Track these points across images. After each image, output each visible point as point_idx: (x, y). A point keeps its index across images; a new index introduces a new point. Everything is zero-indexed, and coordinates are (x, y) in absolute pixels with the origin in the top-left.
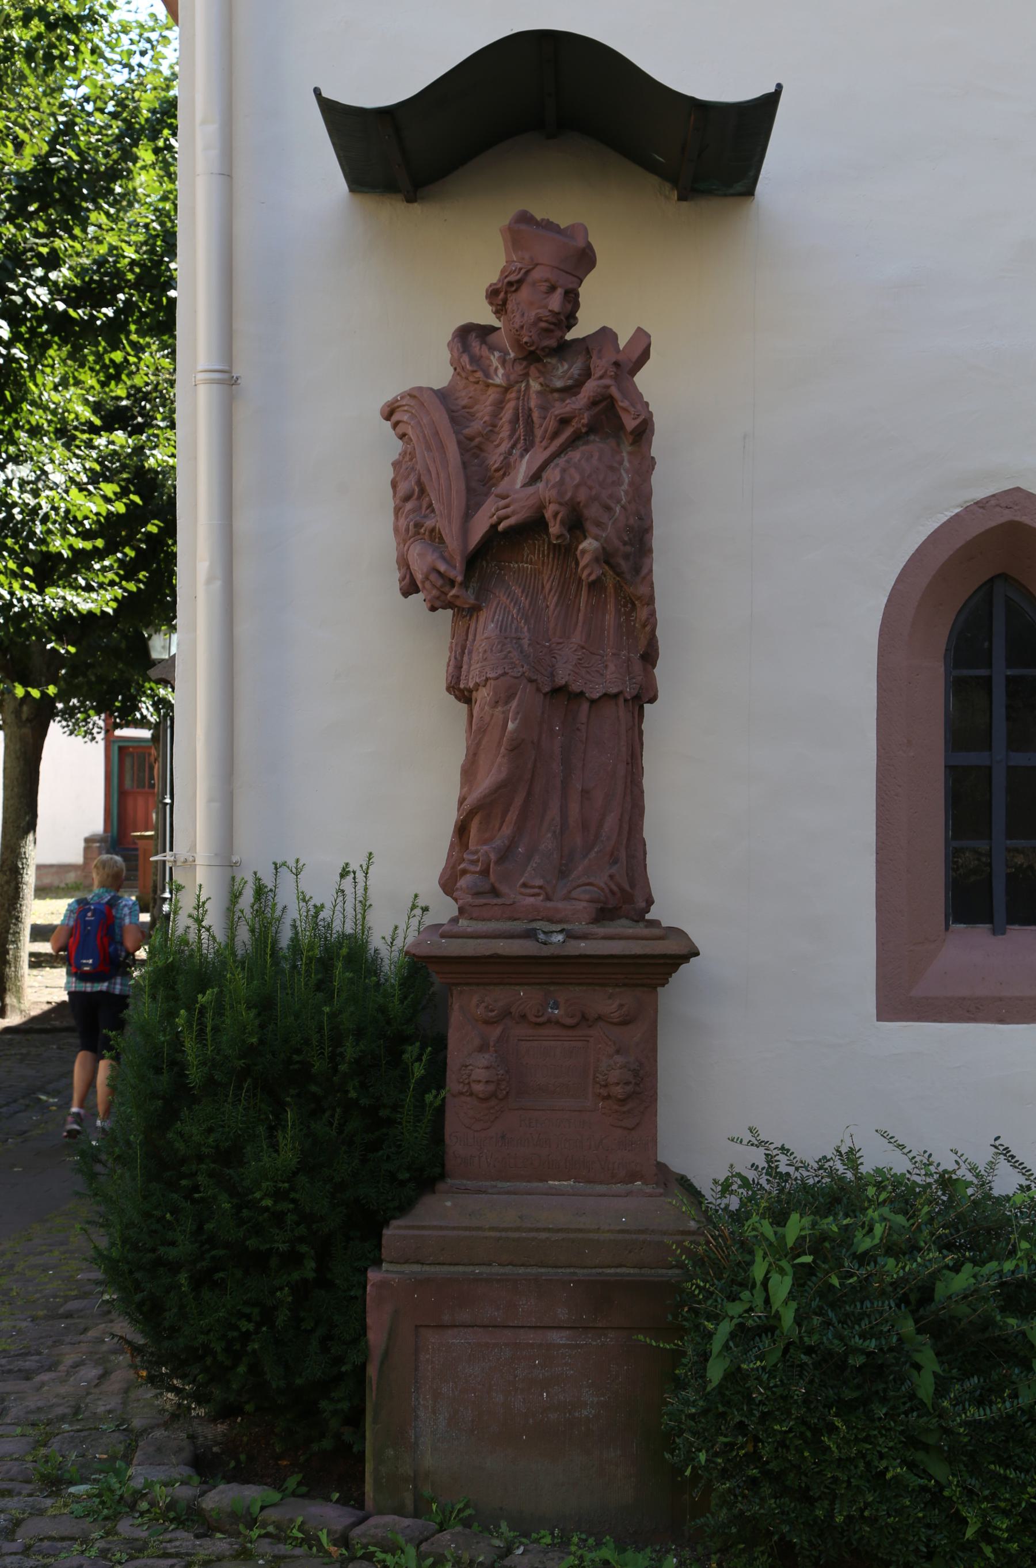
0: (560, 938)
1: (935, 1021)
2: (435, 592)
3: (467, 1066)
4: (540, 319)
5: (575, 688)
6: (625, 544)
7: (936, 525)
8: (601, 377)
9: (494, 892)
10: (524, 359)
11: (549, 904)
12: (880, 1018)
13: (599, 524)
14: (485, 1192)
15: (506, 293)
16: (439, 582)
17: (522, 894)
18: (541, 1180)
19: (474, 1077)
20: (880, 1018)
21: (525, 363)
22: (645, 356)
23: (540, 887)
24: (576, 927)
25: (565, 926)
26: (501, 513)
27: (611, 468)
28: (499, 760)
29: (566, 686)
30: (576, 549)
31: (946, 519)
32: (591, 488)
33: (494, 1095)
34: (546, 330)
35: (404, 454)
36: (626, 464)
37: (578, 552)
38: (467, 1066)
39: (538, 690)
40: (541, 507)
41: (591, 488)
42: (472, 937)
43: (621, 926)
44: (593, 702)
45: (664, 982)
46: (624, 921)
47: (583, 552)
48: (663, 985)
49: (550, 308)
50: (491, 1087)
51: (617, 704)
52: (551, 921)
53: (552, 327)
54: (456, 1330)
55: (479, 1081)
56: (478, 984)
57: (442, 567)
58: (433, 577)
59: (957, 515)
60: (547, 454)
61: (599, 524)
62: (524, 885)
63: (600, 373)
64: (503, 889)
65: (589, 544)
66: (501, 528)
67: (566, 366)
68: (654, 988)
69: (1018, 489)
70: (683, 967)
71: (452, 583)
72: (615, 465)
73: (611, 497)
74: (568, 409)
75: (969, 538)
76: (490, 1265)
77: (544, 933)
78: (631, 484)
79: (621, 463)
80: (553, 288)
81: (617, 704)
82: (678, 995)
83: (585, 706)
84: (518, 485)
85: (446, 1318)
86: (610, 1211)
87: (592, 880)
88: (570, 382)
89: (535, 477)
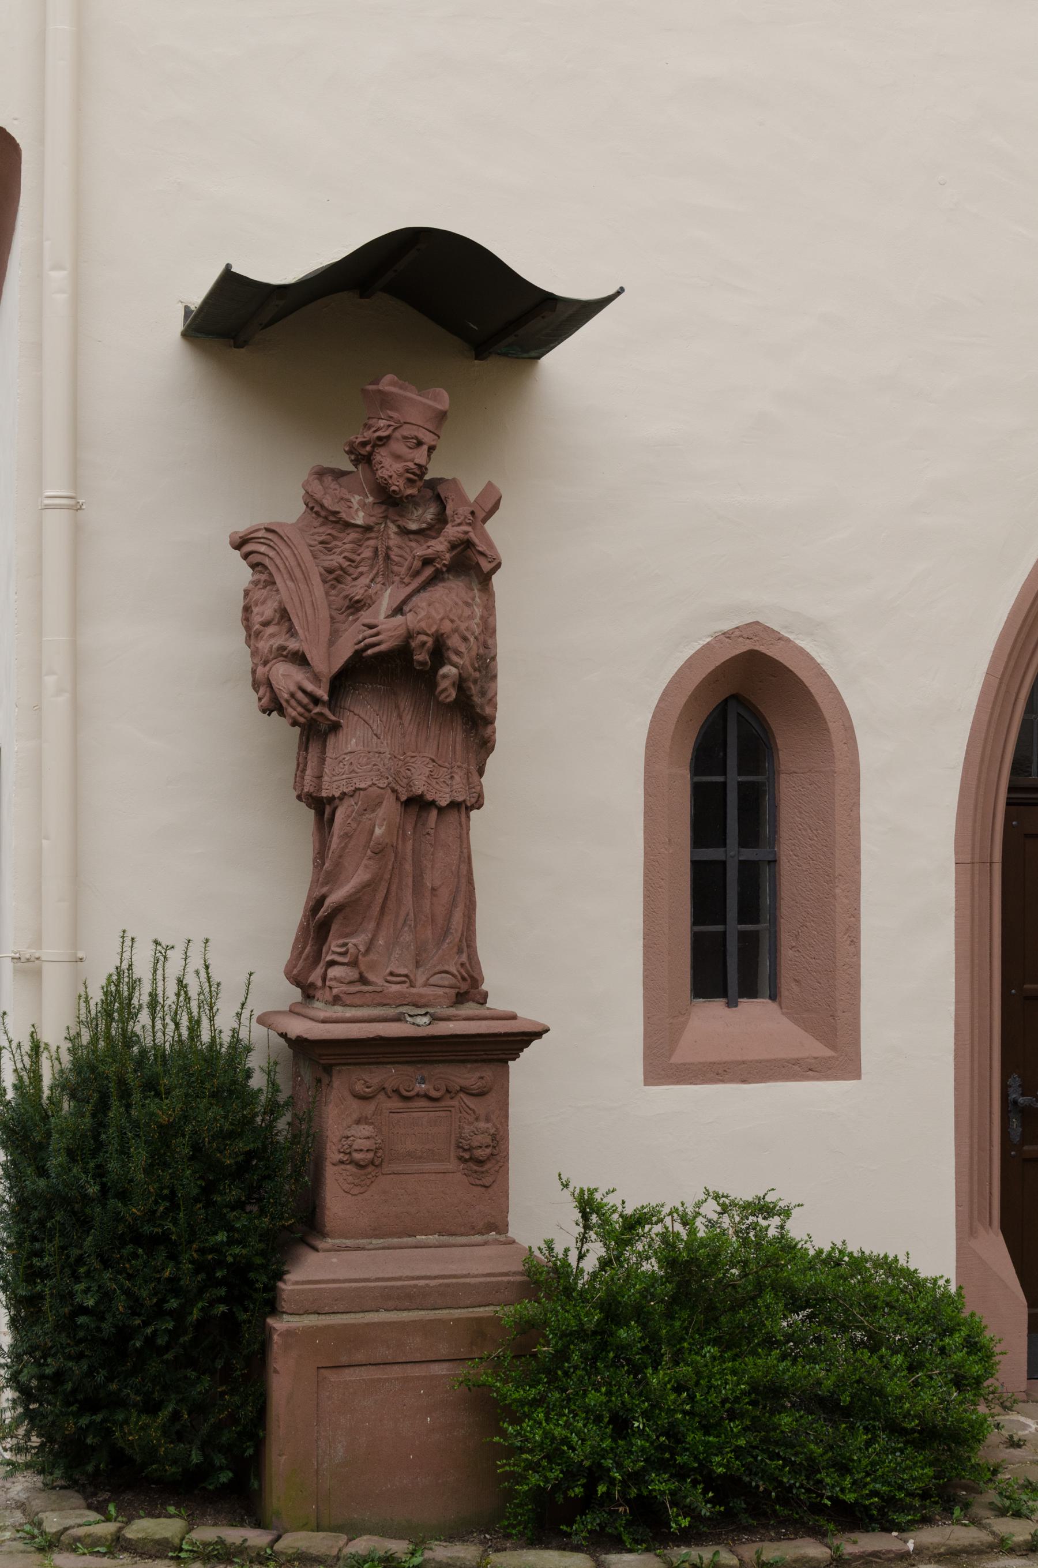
0: (426, 1020)
1: (691, 1084)
2: (300, 709)
3: (348, 1137)
4: (407, 471)
5: (429, 797)
6: (475, 670)
8: (459, 525)
9: (363, 980)
10: (382, 503)
11: (413, 990)
12: (648, 1082)
13: (458, 653)
14: (363, 1249)
15: (373, 447)
16: (305, 700)
17: (388, 982)
18: (410, 1236)
19: (355, 1147)
20: (648, 1082)
21: (384, 507)
22: (496, 507)
23: (406, 976)
24: (438, 1011)
25: (431, 1010)
26: (367, 641)
27: (467, 604)
28: (365, 862)
29: (422, 796)
30: (437, 672)
31: (699, 647)
32: (452, 621)
33: (372, 1163)
34: (410, 480)
35: (256, 583)
36: (477, 599)
37: (438, 678)
38: (348, 1137)
39: (398, 799)
40: (410, 636)
41: (452, 621)
42: (351, 1022)
43: (469, 1009)
44: (441, 810)
45: (515, 1056)
46: (471, 1004)
47: (444, 676)
48: (514, 1059)
49: (417, 461)
50: (370, 1155)
51: (459, 811)
52: (417, 1006)
53: (415, 478)
54: (352, 1369)
55: (361, 1150)
56: (355, 1064)
57: (310, 687)
58: (300, 695)
59: (708, 643)
60: (408, 590)
61: (458, 653)
62: (392, 974)
63: (458, 521)
64: (370, 976)
65: (447, 669)
66: (370, 652)
67: (420, 512)
68: (505, 1062)
69: (757, 623)
70: (535, 1044)
71: (316, 701)
72: (470, 601)
73: (467, 629)
74: (430, 551)
75: (718, 664)
76: (377, 1311)
77: (410, 1016)
78: (482, 617)
79: (473, 599)
80: (420, 443)
81: (459, 811)
82: (522, 1070)
83: (434, 813)
84: (382, 616)
85: (344, 1360)
86: (474, 1261)
87: (446, 968)
88: (424, 525)
89: (399, 610)
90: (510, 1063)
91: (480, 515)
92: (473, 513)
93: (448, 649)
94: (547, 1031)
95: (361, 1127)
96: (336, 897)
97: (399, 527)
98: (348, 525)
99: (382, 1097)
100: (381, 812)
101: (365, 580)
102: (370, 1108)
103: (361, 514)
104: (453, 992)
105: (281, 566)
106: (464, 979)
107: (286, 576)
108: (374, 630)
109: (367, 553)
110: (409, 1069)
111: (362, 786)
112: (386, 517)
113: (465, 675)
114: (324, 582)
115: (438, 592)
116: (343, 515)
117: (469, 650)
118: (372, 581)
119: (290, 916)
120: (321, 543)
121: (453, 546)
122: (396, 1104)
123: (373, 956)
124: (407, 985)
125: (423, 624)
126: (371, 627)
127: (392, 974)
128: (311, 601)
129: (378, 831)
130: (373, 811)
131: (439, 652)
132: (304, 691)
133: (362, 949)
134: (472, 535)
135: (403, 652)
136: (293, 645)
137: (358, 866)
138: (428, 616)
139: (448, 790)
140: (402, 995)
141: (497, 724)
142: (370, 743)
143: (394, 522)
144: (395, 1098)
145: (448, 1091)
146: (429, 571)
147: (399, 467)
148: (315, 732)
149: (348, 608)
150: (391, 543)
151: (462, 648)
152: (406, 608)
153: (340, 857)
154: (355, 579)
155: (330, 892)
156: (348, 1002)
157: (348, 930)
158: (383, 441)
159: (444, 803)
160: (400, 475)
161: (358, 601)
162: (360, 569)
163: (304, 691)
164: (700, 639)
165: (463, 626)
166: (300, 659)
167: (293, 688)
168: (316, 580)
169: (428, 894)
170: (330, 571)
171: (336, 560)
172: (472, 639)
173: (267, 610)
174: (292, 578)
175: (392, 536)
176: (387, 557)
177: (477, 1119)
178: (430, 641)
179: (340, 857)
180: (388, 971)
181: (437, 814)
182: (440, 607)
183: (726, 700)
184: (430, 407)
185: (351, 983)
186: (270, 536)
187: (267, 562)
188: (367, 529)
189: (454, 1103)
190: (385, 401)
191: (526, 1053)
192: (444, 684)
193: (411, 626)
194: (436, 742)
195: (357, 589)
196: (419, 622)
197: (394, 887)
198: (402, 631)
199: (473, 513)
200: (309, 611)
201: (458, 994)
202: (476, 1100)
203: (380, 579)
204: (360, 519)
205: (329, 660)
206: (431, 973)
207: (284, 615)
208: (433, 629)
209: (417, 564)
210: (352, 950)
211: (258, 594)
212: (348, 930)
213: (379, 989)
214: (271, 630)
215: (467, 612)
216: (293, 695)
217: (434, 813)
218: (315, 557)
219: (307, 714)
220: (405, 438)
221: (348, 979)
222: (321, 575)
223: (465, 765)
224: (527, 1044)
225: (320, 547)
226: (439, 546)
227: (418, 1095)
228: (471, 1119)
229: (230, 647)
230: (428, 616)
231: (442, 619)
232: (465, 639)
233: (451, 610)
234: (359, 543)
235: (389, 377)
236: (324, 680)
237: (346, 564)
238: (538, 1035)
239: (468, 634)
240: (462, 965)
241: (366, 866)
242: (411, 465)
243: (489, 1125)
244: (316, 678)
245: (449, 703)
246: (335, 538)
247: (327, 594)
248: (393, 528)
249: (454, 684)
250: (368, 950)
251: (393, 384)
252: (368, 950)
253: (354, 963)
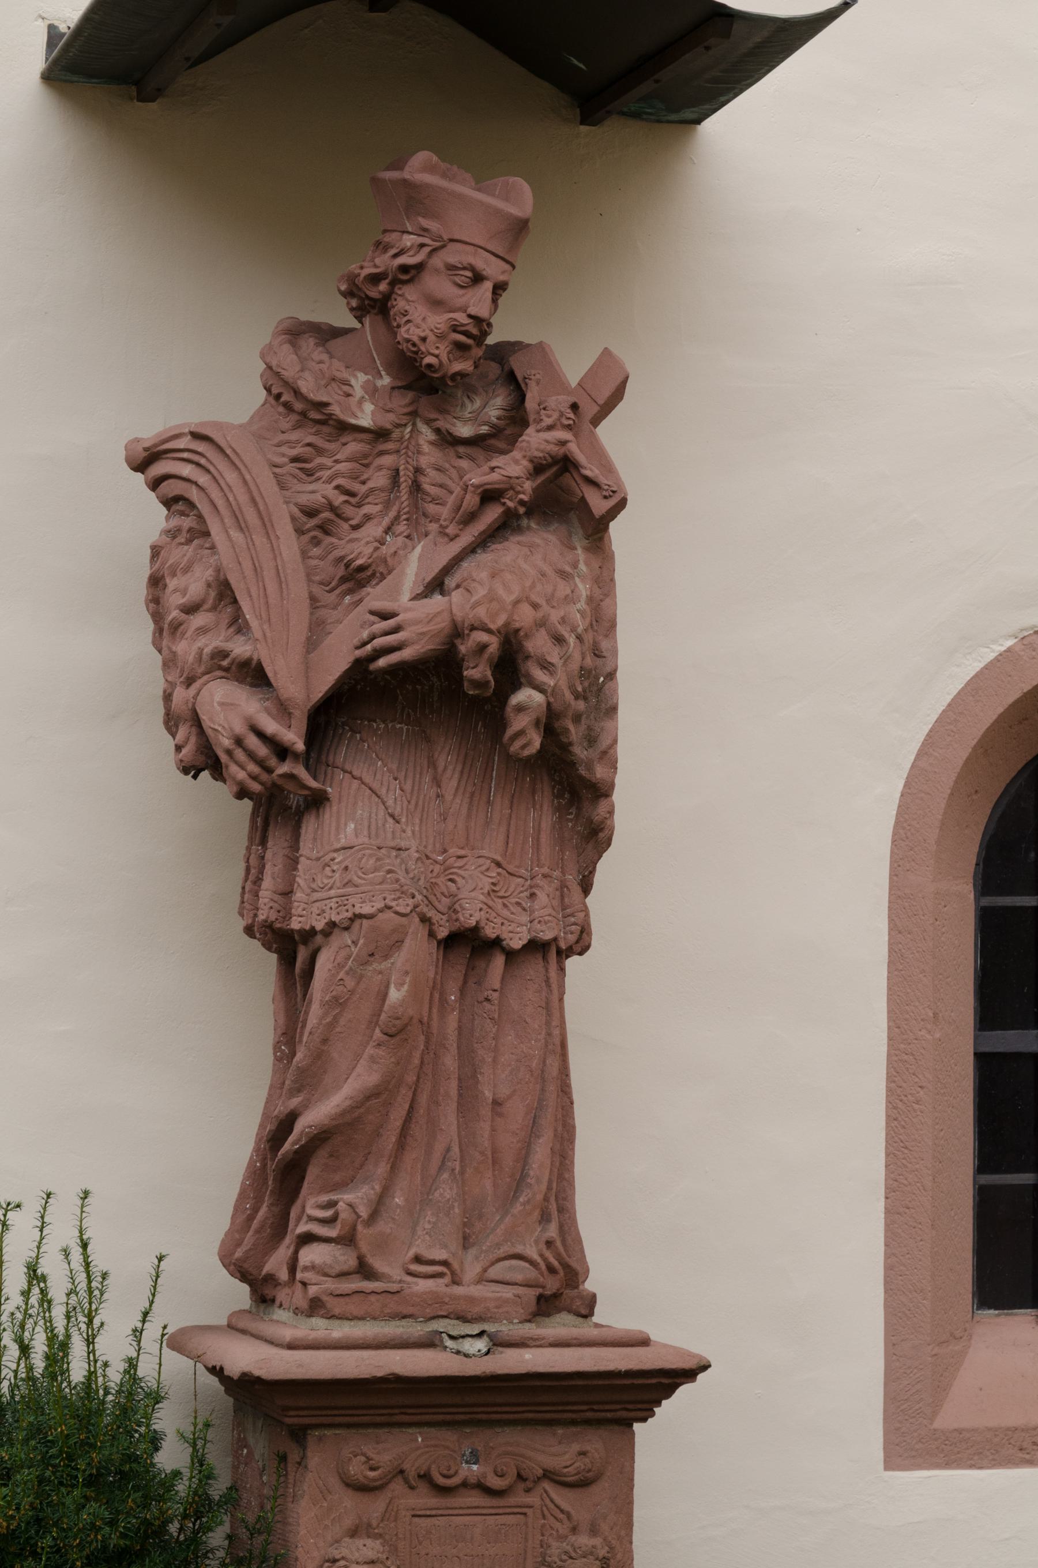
1: (972, 1467)
4: (455, 329)
6: (577, 697)
7: (978, 666)
8: (550, 428)
9: (364, 1270)
10: (407, 387)
11: (458, 1290)
12: (891, 1462)
13: (546, 666)
15: (393, 283)
16: (262, 750)
20: (891, 1462)
21: (410, 395)
23: (445, 1263)
26: (379, 642)
27: (563, 575)
28: (370, 1050)
29: (476, 929)
31: (992, 656)
32: (535, 606)
34: (460, 347)
35: (172, 534)
36: (582, 566)
37: (509, 709)
39: (432, 934)
40: (457, 632)
41: (535, 606)
43: (561, 1326)
44: (511, 955)
45: (646, 1414)
46: (565, 1317)
47: (520, 709)
48: (644, 1420)
49: (472, 311)
51: (545, 958)
52: (463, 1319)
53: (470, 341)
56: (349, 1426)
57: (271, 726)
58: (253, 741)
59: (1009, 650)
61: (546, 666)
63: (548, 421)
64: (378, 1264)
65: (525, 695)
66: (382, 662)
67: (478, 403)
70: (684, 1391)
71: (282, 752)
72: (568, 569)
73: (563, 621)
74: (495, 477)
77: (452, 1337)
78: (590, 600)
79: (575, 565)
80: (478, 278)
81: (545, 958)
82: (658, 1440)
83: (499, 961)
84: (405, 597)
87: (519, 1249)
88: (484, 429)
89: (436, 585)
90: (637, 1427)
91: (589, 410)
92: (574, 407)
93: (528, 657)
94: (705, 1367)
95: (359, 1542)
96: (315, 1116)
97: (438, 431)
98: (344, 428)
99: (397, 1486)
100: (400, 959)
101: (373, 530)
102: (375, 1507)
103: (369, 407)
104: (532, 1293)
105: (220, 503)
106: (551, 1270)
107: (228, 521)
108: (391, 623)
109: (379, 480)
110: (449, 1437)
111: (367, 909)
112: (414, 414)
113: (557, 706)
114: (300, 532)
115: (510, 552)
116: (336, 410)
117: (566, 659)
118: (388, 530)
119: (230, 1150)
120: (295, 460)
121: (538, 468)
122: (424, 1499)
123: (383, 1226)
124: (447, 1280)
125: (481, 612)
126: (384, 616)
127: (418, 1259)
128: (274, 567)
129: (395, 995)
130: (386, 957)
131: (510, 664)
132: (260, 734)
133: (364, 1212)
134: (573, 448)
135: (444, 662)
136: (240, 648)
137: (358, 1057)
138: (492, 597)
139: (525, 918)
140: (437, 1299)
141: (617, 796)
142: (386, 831)
143: (428, 422)
144: (423, 1488)
145: (520, 1476)
146: (492, 514)
147: (439, 321)
148: (280, 809)
149: (343, 580)
150: (424, 461)
151: (554, 655)
152: (450, 582)
153: (325, 1041)
154: (355, 528)
155: (306, 1106)
156: (337, 1311)
157: (337, 1177)
158: (410, 273)
159: (517, 944)
160: (441, 337)
161: (361, 569)
162: (367, 509)
163: (260, 734)
164: (994, 641)
165: (555, 616)
166: (253, 675)
167: (240, 728)
168: (285, 529)
169: (486, 1111)
170: (310, 513)
171: (320, 492)
172: (572, 640)
173: (194, 584)
174: (241, 526)
175: (426, 448)
176: (416, 487)
177: (574, 1530)
178: (494, 644)
179: (325, 1041)
180: (411, 1254)
182: (514, 581)
184: (498, 212)
185: (343, 1275)
186: (201, 447)
187: (194, 495)
188: (380, 434)
189: (533, 1499)
190: (414, 200)
191: (667, 1409)
192: (518, 723)
193: (459, 615)
195: (359, 546)
196: (473, 608)
197: (423, 1099)
198: (442, 624)
199: (574, 407)
200: (272, 587)
201: (540, 1298)
202: (570, 1493)
203: (401, 528)
204: (366, 417)
205: (308, 676)
206: (492, 1257)
207: (224, 592)
208: (501, 621)
209: (472, 500)
210: (345, 1215)
211: (180, 554)
212: (337, 1177)
213: (394, 1287)
214: (200, 619)
215: (563, 589)
216: (239, 742)
217: (499, 961)
218: (282, 486)
219: (265, 777)
220: (451, 268)
221: (338, 1269)
222: (293, 519)
223: (556, 874)
224: (669, 1391)
225: (292, 468)
226: (511, 467)
227: (465, 1484)
228: (563, 1529)
229: (127, 651)
230: (492, 597)
231: (517, 602)
232: (559, 640)
233: (533, 586)
234: (363, 461)
235: (422, 157)
236: (297, 713)
237: (339, 499)
238: (689, 1375)
239: (564, 631)
240: (549, 1243)
241: (373, 1059)
242: (462, 318)
243: (597, 1541)
244: (283, 710)
245: (529, 758)
246: (320, 451)
247: (304, 555)
248: (426, 434)
249: (537, 723)
250: (374, 1215)
251: (431, 169)
252: (374, 1215)
253: (348, 1239)
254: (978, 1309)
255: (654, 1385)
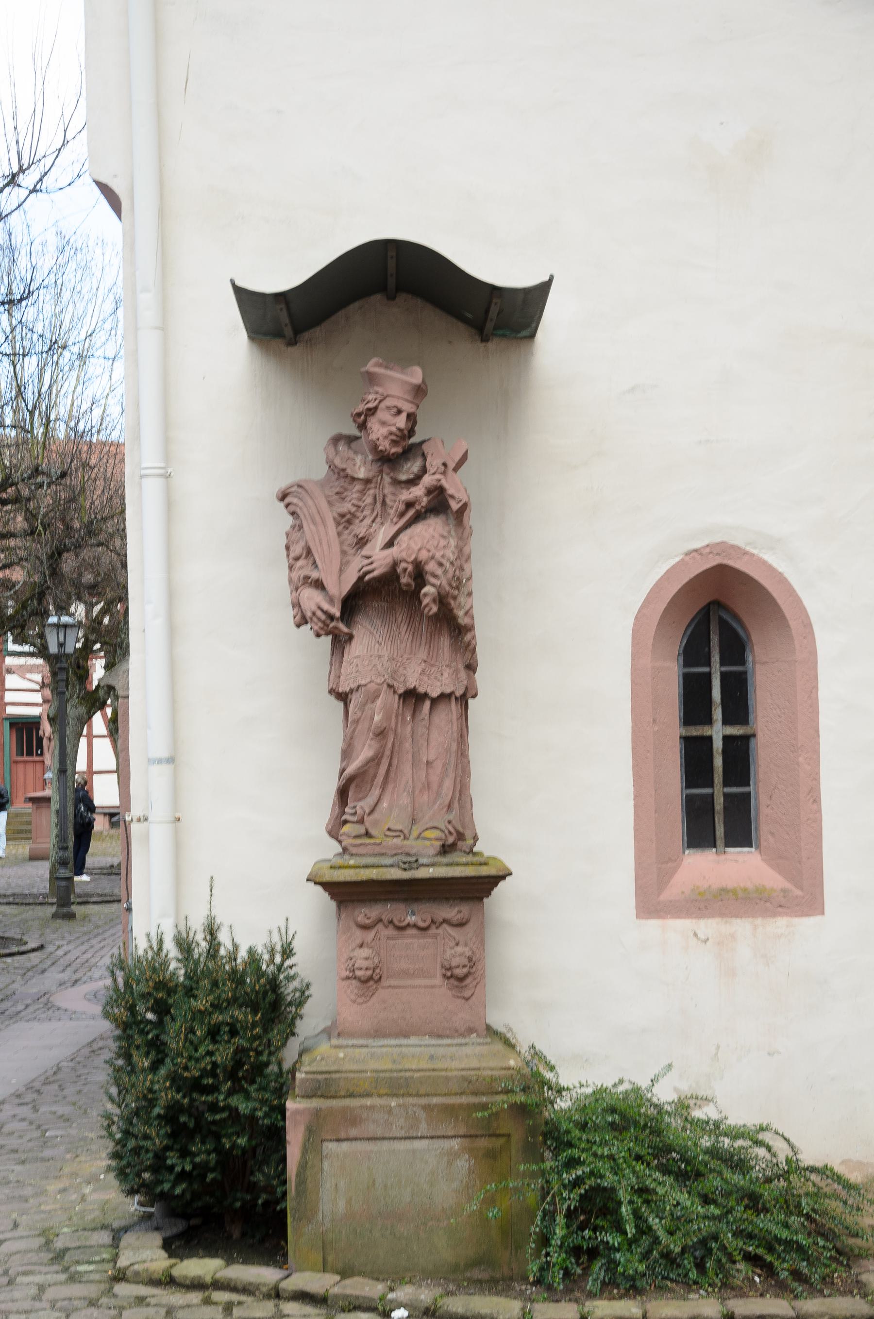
2: (320, 624)
4: (391, 433)
5: (421, 690)
7: (668, 567)
8: (434, 474)
9: (367, 834)
11: (406, 842)
13: (435, 576)
15: (366, 416)
16: (323, 617)
21: (379, 464)
23: (401, 831)
26: (365, 569)
28: (368, 742)
30: (420, 592)
32: (429, 551)
33: (371, 978)
35: (293, 527)
39: (395, 692)
40: (395, 564)
41: (429, 551)
47: (425, 595)
49: (398, 425)
50: (369, 973)
57: (326, 606)
58: (319, 613)
61: (435, 576)
62: (389, 829)
63: (432, 471)
64: (373, 831)
65: (426, 589)
66: (367, 578)
67: (409, 465)
68: (481, 899)
69: (723, 543)
70: (502, 884)
71: (332, 618)
73: (443, 556)
75: (692, 576)
78: (457, 547)
80: (399, 412)
85: (343, 1135)
87: (436, 824)
88: (412, 476)
89: (390, 544)
90: (485, 900)
91: (451, 465)
92: (445, 465)
93: (426, 573)
94: (511, 874)
95: (362, 950)
96: (351, 770)
97: (391, 478)
98: (354, 479)
99: (380, 926)
100: (379, 702)
101: (368, 521)
102: (371, 934)
103: (363, 469)
104: (438, 844)
105: (307, 514)
106: (450, 833)
107: (310, 521)
108: (369, 561)
109: (369, 500)
110: (401, 906)
111: (363, 682)
112: (381, 472)
113: (443, 593)
114: (338, 524)
115: (419, 529)
116: (349, 471)
117: (445, 572)
118: (373, 521)
119: (332, 785)
120: (337, 493)
121: (429, 492)
122: (391, 931)
123: (375, 816)
124: (402, 837)
125: (404, 555)
126: (368, 557)
127: (389, 829)
128: (326, 539)
129: (377, 718)
130: (373, 702)
131: (419, 575)
132: (322, 610)
133: (367, 811)
134: (444, 483)
135: (391, 576)
136: (315, 575)
137: (364, 745)
138: (408, 548)
139: (439, 684)
140: (397, 847)
141: (478, 631)
142: (374, 648)
143: (388, 474)
144: (391, 927)
145: (433, 922)
146: (411, 513)
147: (384, 431)
148: (340, 643)
149: (356, 544)
150: (386, 491)
151: (439, 572)
152: (396, 543)
153: (351, 738)
154: (362, 521)
155: (347, 765)
156: (354, 852)
157: (361, 795)
158: (372, 411)
159: (435, 694)
160: (386, 437)
161: (362, 538)
162: (364, 513)
163: (322, 610)
164: (676, 556)
165: (438, 555)
166: (319, 585)
167: (314, 608)
168: (331, 524)
169: (424, 766)
170: (342, 516)
171: (347, 507)
172: (448, 565)
173: (297, 549)
174: (314, 522)
175: (387, 485)
176: (384, 503)
177: (457, 944)
178: (410, 568)
179: (351, 738)
180: (386, 828)
181: (439, 706)
182: (426, 539)
183: (709, 604)
184: (406, 382)
185: (357, 837)
186: (300, 490)
187: (298, 511)
188: (367, 481)
189: (440, 931)
190: (371, 379)
191: (496, 891)
192: (425, 601)
193: (396, 557)
194: (427, 647)
195: (360, 529)
196: (401, 552)
197: (395, 762)
198: (389, 560)
199: (445, 465)
200: (325, 547)
201: (443, 846)
202: (456, 929)
203: (378, 519)
204: (362, 474)
205: (340, 585)
206: (424, 828)
207: (309, 552)
208: (413, 558)
209: (402, 507)
210: (359, 811)
211: (296, 535)
212: (361, 795)
213: (378, 841)
214: (300, 563)
215: (443, 542)
216: (314, 614)
217: (427, 704)
218: (330, 503)
219: (325, 628)
220: (388, 408)
221: (353, 834)
222: (334, 519)
223: (454, 664)
224: (496, 884)
225: (336, 497)
226: (418, 492)
227: (408, 925)
228: (452, 944)
229: (279, 579)
230: (408, 548)
231: (419, 550)
232: (441, 564)
233: (428, 541)
234: (363, 492)
235: (374, 360)
236: (336, 601)
237: (353, 509)
238: (503, 877)
239: (444, 561)
240: (449, 822)
241: (370, 745)
242: (394, 429)
243: (467, 950)
244: (331, 601)
245: (432, 616)
246: (346, 490)
247: (339, 534)
248: (387, 479)
249: (434, 601)
250: (371, 812)
251: (380, 365)
252: (371, 812)
253: (361, 821)
254: (688, 847)
255: (493, 881)
